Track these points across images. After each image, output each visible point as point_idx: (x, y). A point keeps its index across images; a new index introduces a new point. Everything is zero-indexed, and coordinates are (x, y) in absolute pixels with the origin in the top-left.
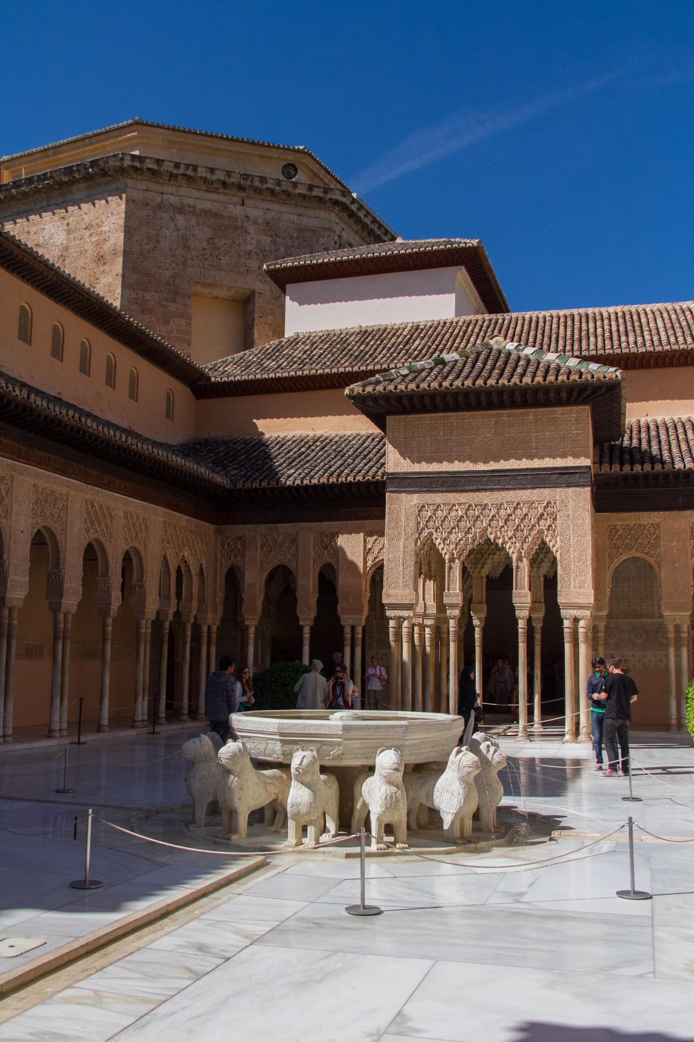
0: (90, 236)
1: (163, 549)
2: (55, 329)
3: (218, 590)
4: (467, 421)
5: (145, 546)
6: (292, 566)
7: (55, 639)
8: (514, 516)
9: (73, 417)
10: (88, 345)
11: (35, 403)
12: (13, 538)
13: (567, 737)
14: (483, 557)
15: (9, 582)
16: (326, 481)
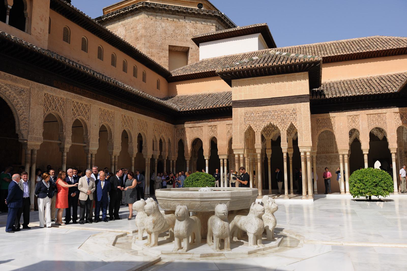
0: (133, 31)
1: (154, 133)
3: (176, 148)
4: (262, 80)
6: (200, 138)
8: (280, 115)
10: (126, 62)
11: (97, 76)
12: (91, 128)
13: (303, 197)
15: (90, 144)
16: (212, 107)
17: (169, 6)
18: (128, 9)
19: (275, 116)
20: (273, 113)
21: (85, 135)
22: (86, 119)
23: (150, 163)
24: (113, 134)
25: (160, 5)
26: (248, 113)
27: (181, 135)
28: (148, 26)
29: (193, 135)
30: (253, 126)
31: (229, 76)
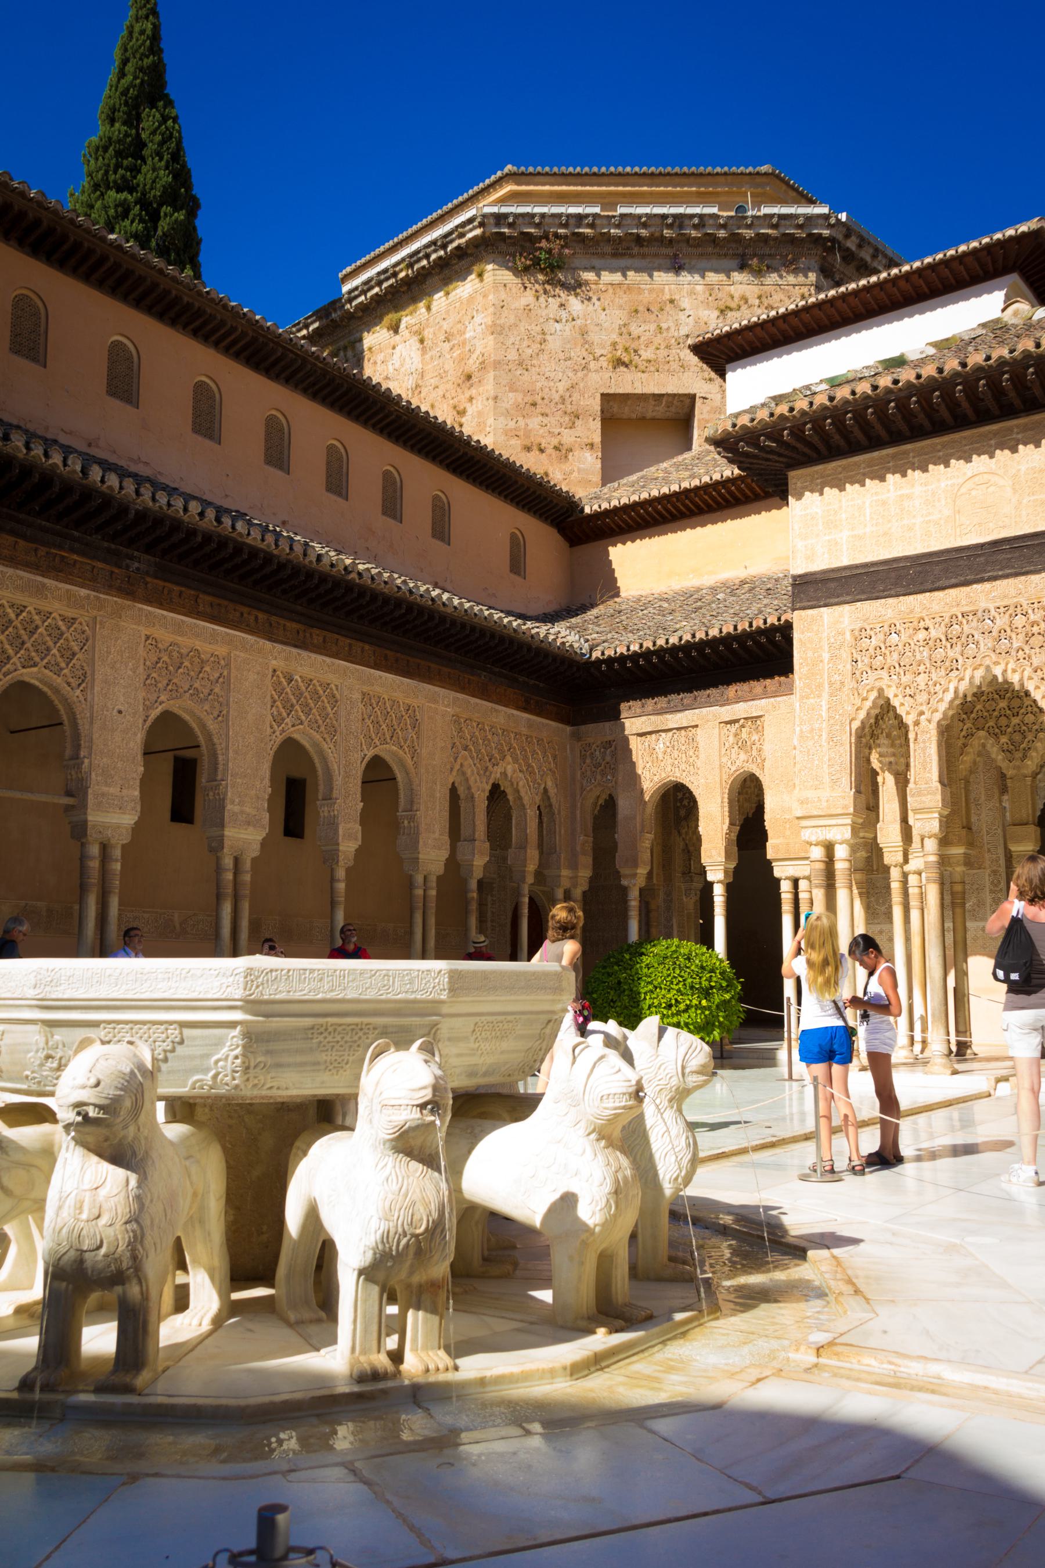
2: (387, 476)
3: (579, 829)
4: (941, 454)
5: (414, 753)
7: (219, 897)
9: (202, 514)
10: (343, 450)
11: (103, 481)
14: (1025, 737)
15: (90, 797)
16: (731, 630)
17: (598, 222)
18: (427, 256)
19: (1014, 636)
20: (1002, 621)
21: (71, 759)
22: (69, 684)
23: (434, 899)
24: (220, 758)
25: (557, 221)
26: (872, 633)
27: (603, 774)
28: (512, 319)
29: (654, 770)
30: (896, 696)
31: (771, 451)
